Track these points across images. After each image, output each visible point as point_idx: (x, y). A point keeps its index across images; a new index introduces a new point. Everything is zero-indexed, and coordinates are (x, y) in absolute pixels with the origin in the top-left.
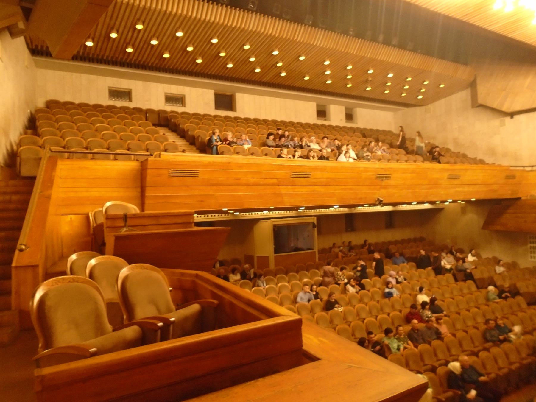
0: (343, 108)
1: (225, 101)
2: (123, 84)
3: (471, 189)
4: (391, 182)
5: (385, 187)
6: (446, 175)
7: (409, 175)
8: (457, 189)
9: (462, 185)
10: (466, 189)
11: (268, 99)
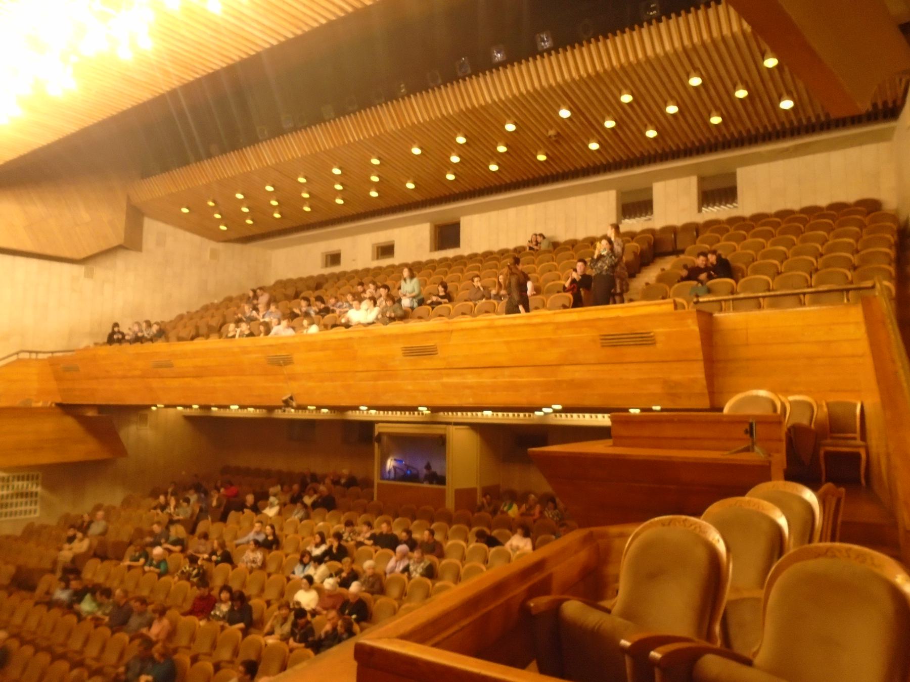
0: (694, 180)
1: (447, 235)
2: (333, 245)
3: (486, 378)
4: (298, 368)
5: (292, 377)
6: (397, 349)
7: (321, 354)
8: (445, 380)
9: (452, 369)
10: (471, 379)
11: (512, 212)
